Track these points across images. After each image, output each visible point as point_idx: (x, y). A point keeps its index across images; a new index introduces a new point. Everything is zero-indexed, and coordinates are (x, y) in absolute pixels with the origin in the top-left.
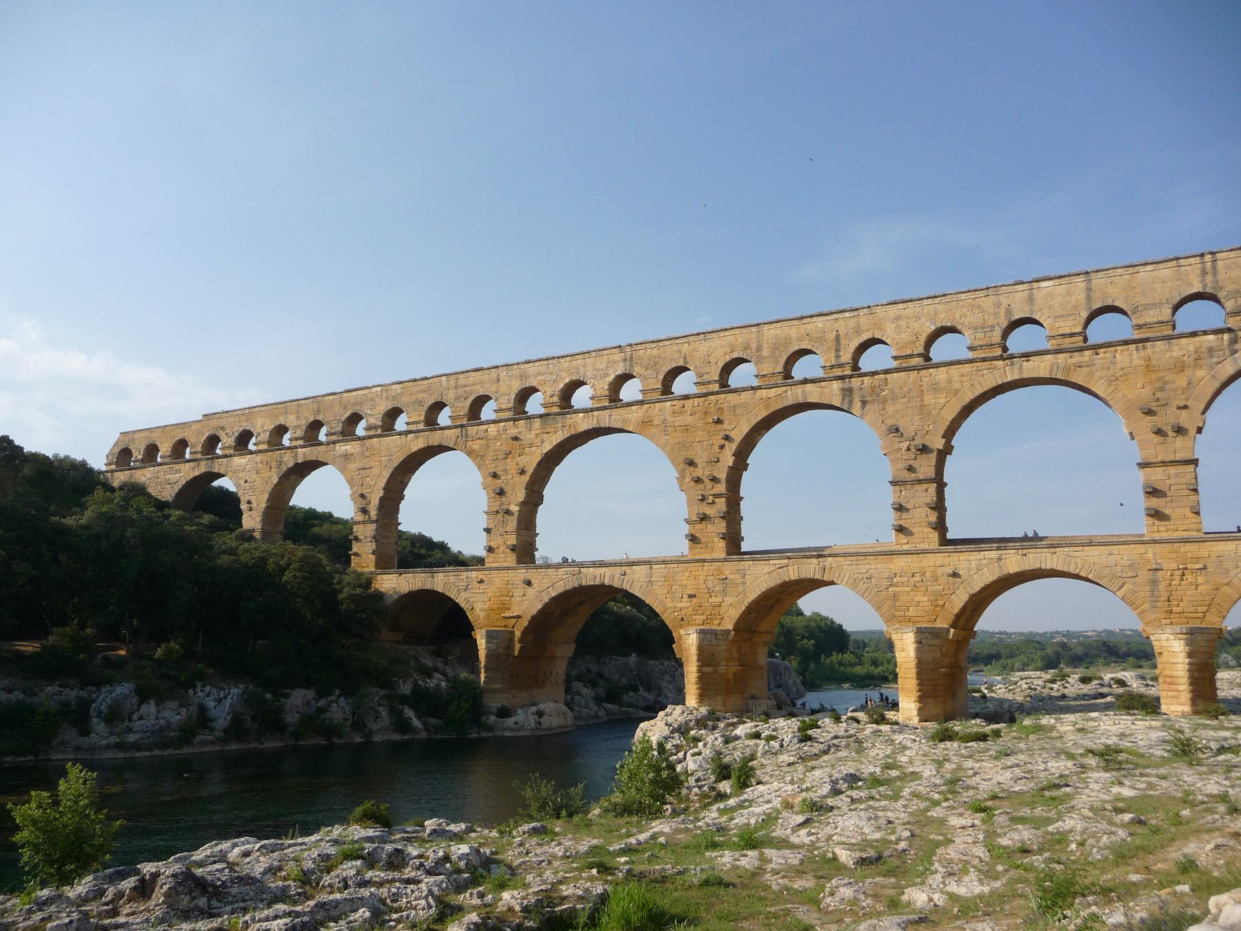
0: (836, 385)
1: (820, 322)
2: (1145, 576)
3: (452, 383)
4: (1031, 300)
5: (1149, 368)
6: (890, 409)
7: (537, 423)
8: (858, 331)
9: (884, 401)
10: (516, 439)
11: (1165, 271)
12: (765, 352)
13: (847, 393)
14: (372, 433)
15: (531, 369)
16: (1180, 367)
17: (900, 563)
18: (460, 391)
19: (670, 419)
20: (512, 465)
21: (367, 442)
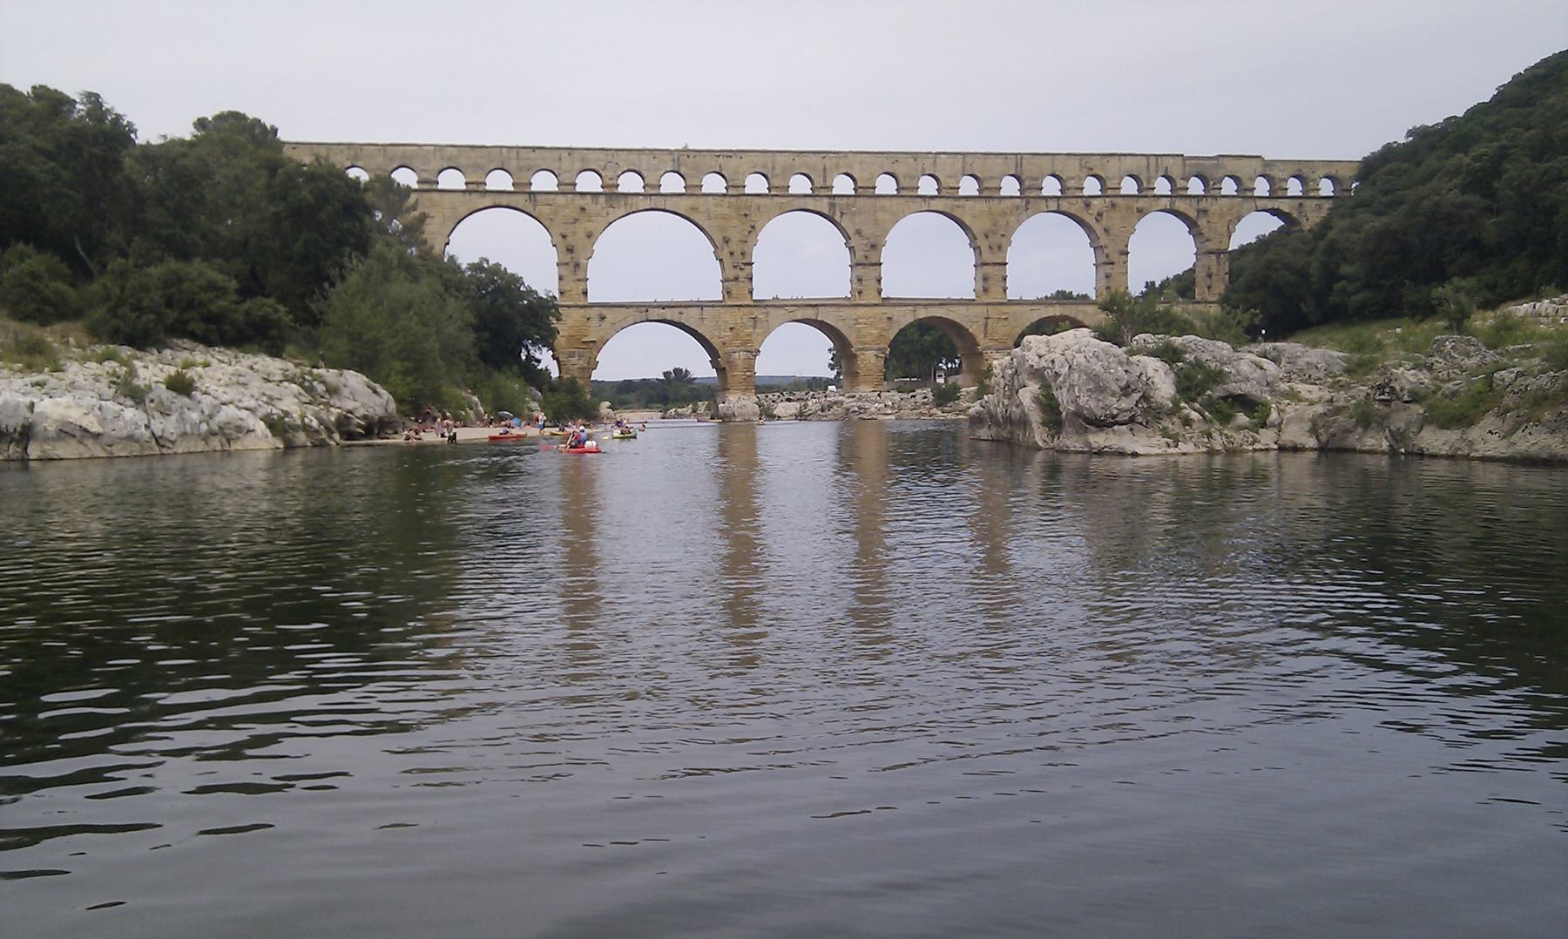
0: (826, 200)
1: (814, 158)
2: (982, 321)
3: (513, 154)
4: (935, 163)
5: (990, 213)
6: (857, 220)
7: (602, 199)
8: (837, 166)
9: (854, 214)
10: (583, 209)
11: (1000, 160)
12: (778, 171)
13: (832, 206)
14: (426, 187)
15: (592, 155)
16: (1004, 214)
17: (861, 311)
18: (522, 163)
19: (713, 209)
20: (581, 229)
21: (427, 195)
